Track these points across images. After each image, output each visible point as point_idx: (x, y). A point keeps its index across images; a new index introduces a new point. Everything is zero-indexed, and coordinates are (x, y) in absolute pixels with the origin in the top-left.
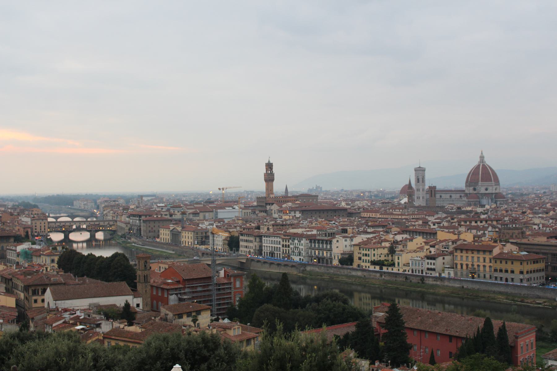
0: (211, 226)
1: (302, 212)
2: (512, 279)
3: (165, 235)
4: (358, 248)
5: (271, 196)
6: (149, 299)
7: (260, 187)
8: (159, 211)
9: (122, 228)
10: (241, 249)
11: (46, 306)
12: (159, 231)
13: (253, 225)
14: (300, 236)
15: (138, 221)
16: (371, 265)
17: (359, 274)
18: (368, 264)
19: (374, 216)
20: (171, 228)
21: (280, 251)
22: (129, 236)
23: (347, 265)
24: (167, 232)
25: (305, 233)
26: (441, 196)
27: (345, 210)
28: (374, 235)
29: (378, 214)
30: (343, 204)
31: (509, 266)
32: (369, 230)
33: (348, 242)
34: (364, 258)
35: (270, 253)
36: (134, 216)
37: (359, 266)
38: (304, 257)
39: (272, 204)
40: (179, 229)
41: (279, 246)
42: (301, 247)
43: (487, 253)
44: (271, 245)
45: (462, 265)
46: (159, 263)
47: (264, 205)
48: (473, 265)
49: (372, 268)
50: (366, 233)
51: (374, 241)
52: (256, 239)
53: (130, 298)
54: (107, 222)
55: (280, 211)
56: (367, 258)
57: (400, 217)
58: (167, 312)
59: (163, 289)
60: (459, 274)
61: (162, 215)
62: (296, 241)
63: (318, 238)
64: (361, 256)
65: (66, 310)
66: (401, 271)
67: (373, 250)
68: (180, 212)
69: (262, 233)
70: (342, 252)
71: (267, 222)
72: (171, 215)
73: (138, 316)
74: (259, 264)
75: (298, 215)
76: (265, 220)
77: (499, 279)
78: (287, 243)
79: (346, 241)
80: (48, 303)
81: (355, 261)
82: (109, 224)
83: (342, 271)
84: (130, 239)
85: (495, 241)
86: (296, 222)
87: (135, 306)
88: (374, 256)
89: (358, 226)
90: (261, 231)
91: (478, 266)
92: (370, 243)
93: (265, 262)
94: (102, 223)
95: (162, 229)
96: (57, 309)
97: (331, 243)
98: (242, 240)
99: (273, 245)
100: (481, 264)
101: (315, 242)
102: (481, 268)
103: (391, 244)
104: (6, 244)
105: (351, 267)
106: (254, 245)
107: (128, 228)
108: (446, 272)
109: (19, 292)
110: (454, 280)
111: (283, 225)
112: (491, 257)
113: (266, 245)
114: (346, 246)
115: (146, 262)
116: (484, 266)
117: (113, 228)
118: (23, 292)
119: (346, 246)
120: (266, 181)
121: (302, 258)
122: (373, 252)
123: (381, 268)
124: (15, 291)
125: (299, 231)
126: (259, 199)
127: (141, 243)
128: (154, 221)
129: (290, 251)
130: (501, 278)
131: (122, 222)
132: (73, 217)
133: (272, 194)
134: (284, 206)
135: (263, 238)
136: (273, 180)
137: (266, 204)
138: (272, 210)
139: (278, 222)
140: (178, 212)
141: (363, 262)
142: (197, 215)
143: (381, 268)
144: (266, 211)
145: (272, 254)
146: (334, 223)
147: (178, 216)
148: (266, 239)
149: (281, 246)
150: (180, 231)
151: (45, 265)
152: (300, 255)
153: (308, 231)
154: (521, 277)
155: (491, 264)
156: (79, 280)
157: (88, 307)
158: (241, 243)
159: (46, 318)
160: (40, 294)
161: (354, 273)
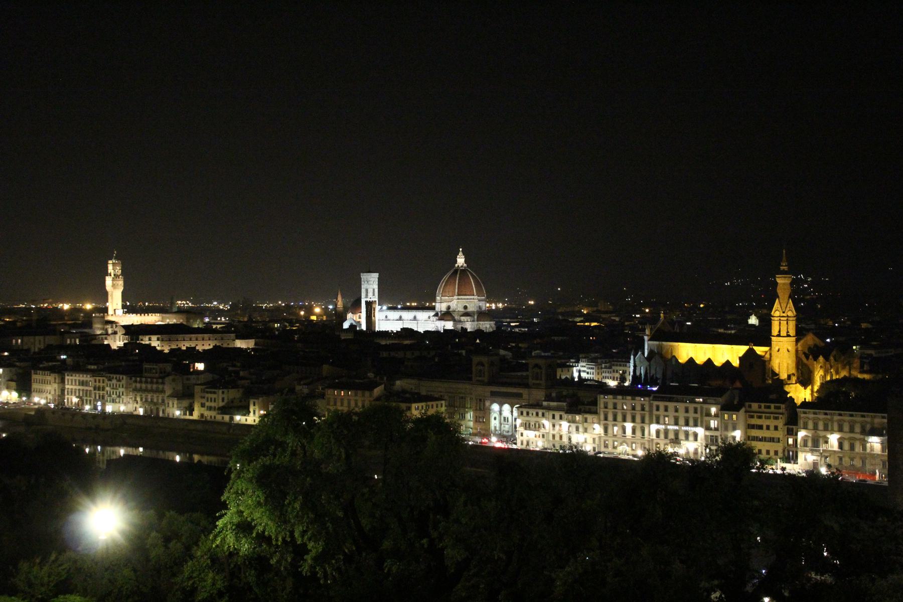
26: (401, 317)
34: (208, 404)
43: (367, 393)
62: (114, 381)
78: (101, 384)
79: (188, 379)
88: (223, 400)
97: (163, 383)
101: (141, 382)
103: (252, 383)
112: (372, 399)
129: (106, 396)
135: (67, 377)
143: (232, 419)
148: (70, 378)
149: (92, 389)
158: (35, 386)
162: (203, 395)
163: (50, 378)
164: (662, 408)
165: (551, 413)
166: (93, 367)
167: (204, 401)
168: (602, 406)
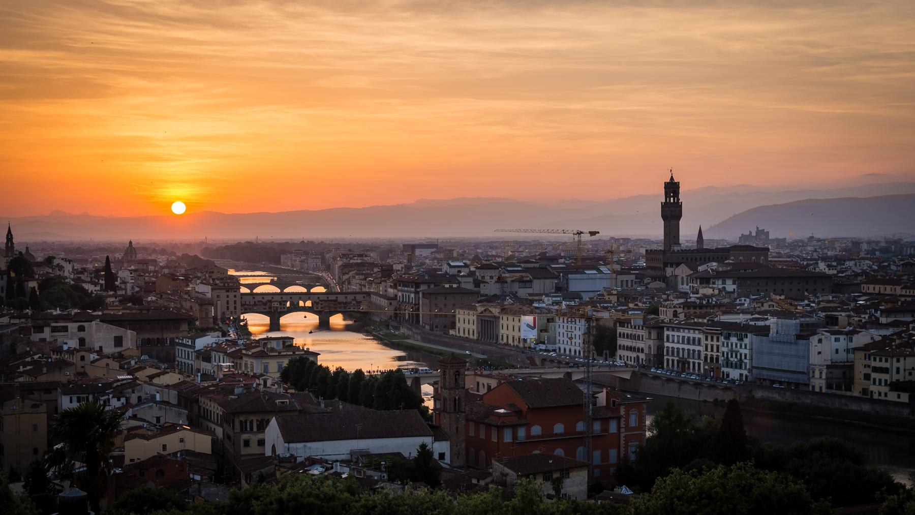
0: (556, 307)
1: (738, 280)
3: (466, 323)
4: (861, 355)
5: (676, 248)
6: (463, 445)
7: (655, 231)
8: (454, 276)
9: (381, 308)
10: (620, 352)
11: (268, 453)
12: (454, 316)
13: (640, 304)
14: (741, 330)
15: (412, 295)
16: (891, 390)
17: (866, 407)
18: (886, 389)
19: (888, 291)
21: (699, 358)
22: (395, 324)
23: (839, 388)
24: (473, 317)
25: (752, 323)
27: (829, 277)
28: (897, 330)
29: (898, 288)
30: (822, 266)
32: (883, 320)
33: (842, 344)
34: (874, 375)
35: (678, 362)
36: (406, 283)
37: (865, 391)
38: (750, 371)
39: (678, 265)
40: (495, 311)
41: (697, 348)
42: (743, 351)
44: (681, 346)
46: (476, 375)
47: (662, 266)
49: (892, 396)
50: (876, 324)
51: (898, 342)
52: (650, 333)
53: (428, 440)
54: (352, 297)
55: (692, 278)
56: (884, 377)
58: (507, 470)
59: (489, 426)
61: (459, 283)
62: (734, 340)
64: (869, 371)
65: (312, 461)
67: (895, 360)
68: (495, 279)
69: (663, 321)
70: (829, 363)
71: (667, 300)
72: (477, 283)
73: (444, 476)
74: (658, 382)
75: (730, 286)
76: (664, 297)
79: (837, 340)
80: (274, 446)
81: (856, 381)
82: (355, 299)
84: (397, 329)
86: (726, 301)
87: (436, 456)
89: (859, 310)
90: (662, 317)
92: (891, 347)
93: (669, 380)
94: (341, 298)
95: (462, 311)
96: (293, 458)
98: (623, 336)
99: (686, 347)
104: (174, 335)
105: (848, 393)
106: (647, 343)
107: (392, 308)
109: (213, 426)
111: (701, 306)
113: (670, 345)
114: (837, 351)
115: (458, 374)
117: (363, 308)
118: (222, 426)
119: (837, 351)
120: (664, 217)
121: (745, 372)
122: (896, 365)
124: (206, 423)
125: (740, 318)
126: (651, 254)
127: (419, 337)
131: (381, 296)
132: (282, 284)
133: (677, 243)
134: (700, 268)
135: (666, 333)
136: (679, 216)
137: (666, 265)
138: (676, 276)
139: (693, 300)
140: (491, 277)
141: (874, 383)
142: (528, 284)
144: (664, 279)
145: (684, 364)
146: (808, 305)
147: (492, 288)
148: (671, 333)
149: (702, 349)
150: (497, 314)
151: (262, 375)
152: (741, 368)
153: (758, 319)
156: (326, 406)
157: (347, 457)
158: (621, 342)
159: (275, 475)
160: (255, 429)
161: (854, 407)
162: (867, 362)
166: (700, 320)
167: (869, 371)
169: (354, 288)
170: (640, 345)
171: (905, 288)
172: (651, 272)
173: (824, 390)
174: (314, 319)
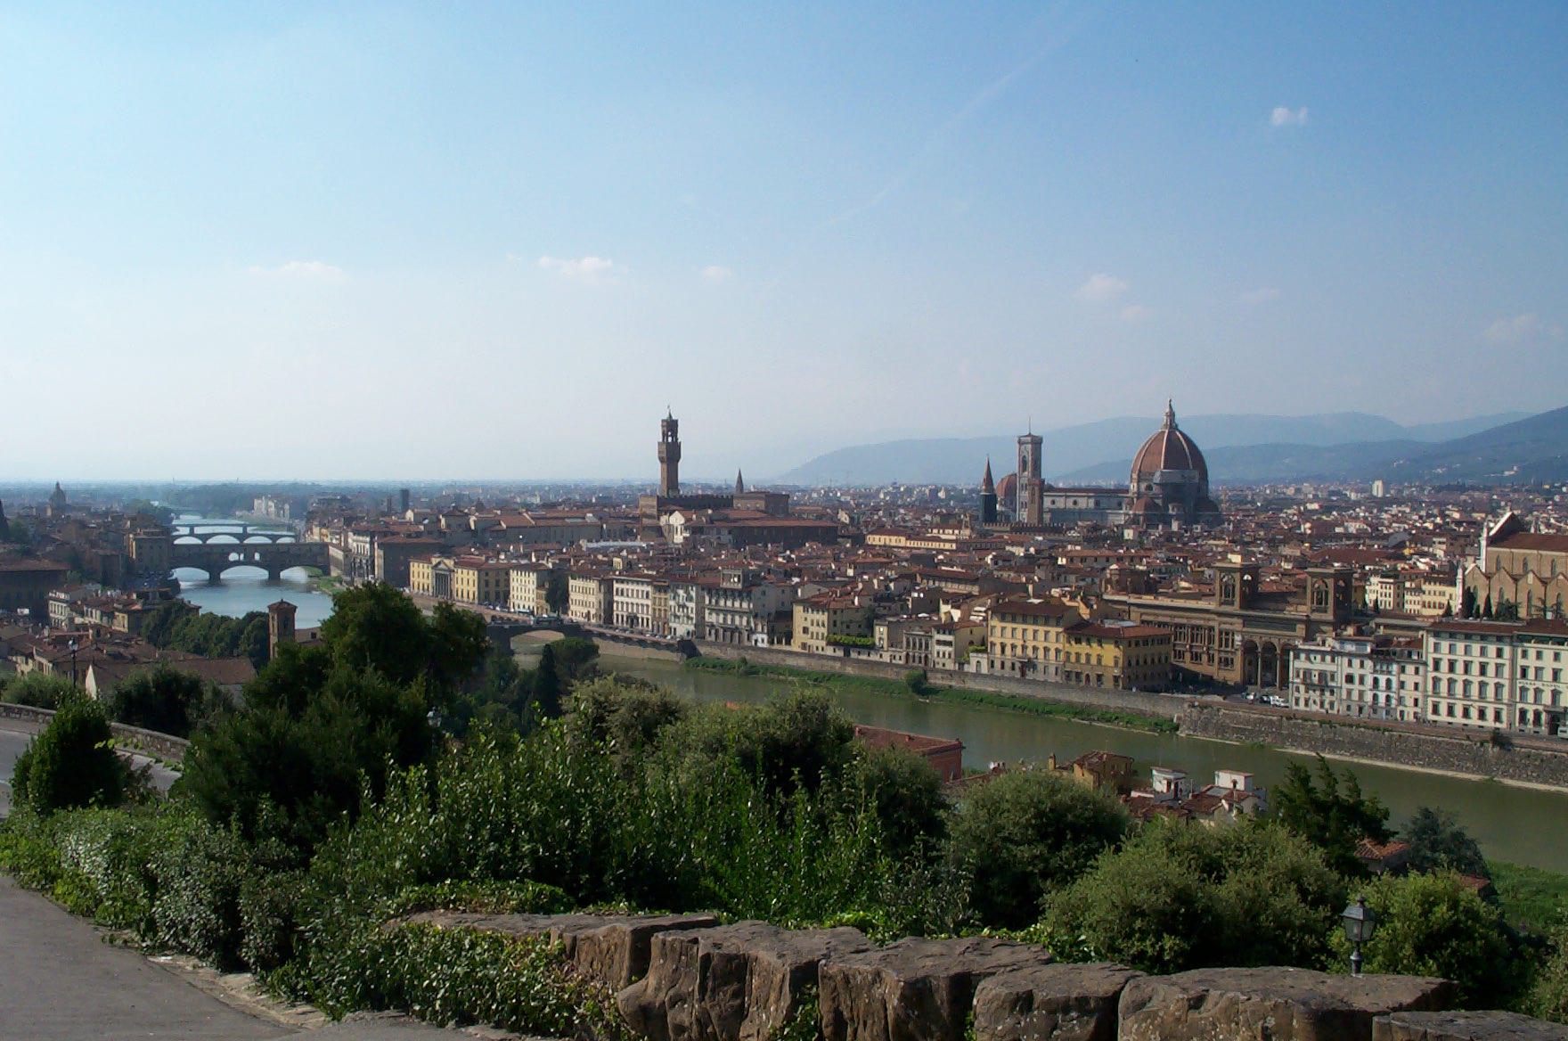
2: (1099, 677)
7: (650, 472)
9: (337, 563)
10: (573, 607)
17: (801, 662)
20: (435, 561)
23: (779, 642)
30: (844, 517)
31: (1095, 649)
37: (804, 646)
39: (671, 513)
45: (1003, 647)
47: (654, 512)
48: (1024, 648)
49: (829, 651)
57: (948, 546)
60: (997, 664)
62: (681, 592)
63: (725, 585)
64: (808, 624)
66: (886, 658)
75: (726, 537)
77: (1073, 676)
83: (766, 656)
85: (1073, 598)
91: (1035, 649)
100: (1041, 645)
102: (1041, 653)
108: (973, 661)
110: (991, 676)
116: (1046, 650)
123: (847, 654)
128: (402, 547)
130: (1078, 675)
135: (616, 585)
143: (847, 654)
148: (620, 586)
149: (649, 602)
154: (1117, 672)
155: (1060, 646)
158: (573, 596)
161: (791, 661)
163: (593, 585)
164: (1532, 653)
165: (1346, 660)
168: (1431, 649)
169: (316, 538)
170: (592, 599)
171: (909, 538)
172: (646, 521)
173: (765, 645)
174: (264, 574)
